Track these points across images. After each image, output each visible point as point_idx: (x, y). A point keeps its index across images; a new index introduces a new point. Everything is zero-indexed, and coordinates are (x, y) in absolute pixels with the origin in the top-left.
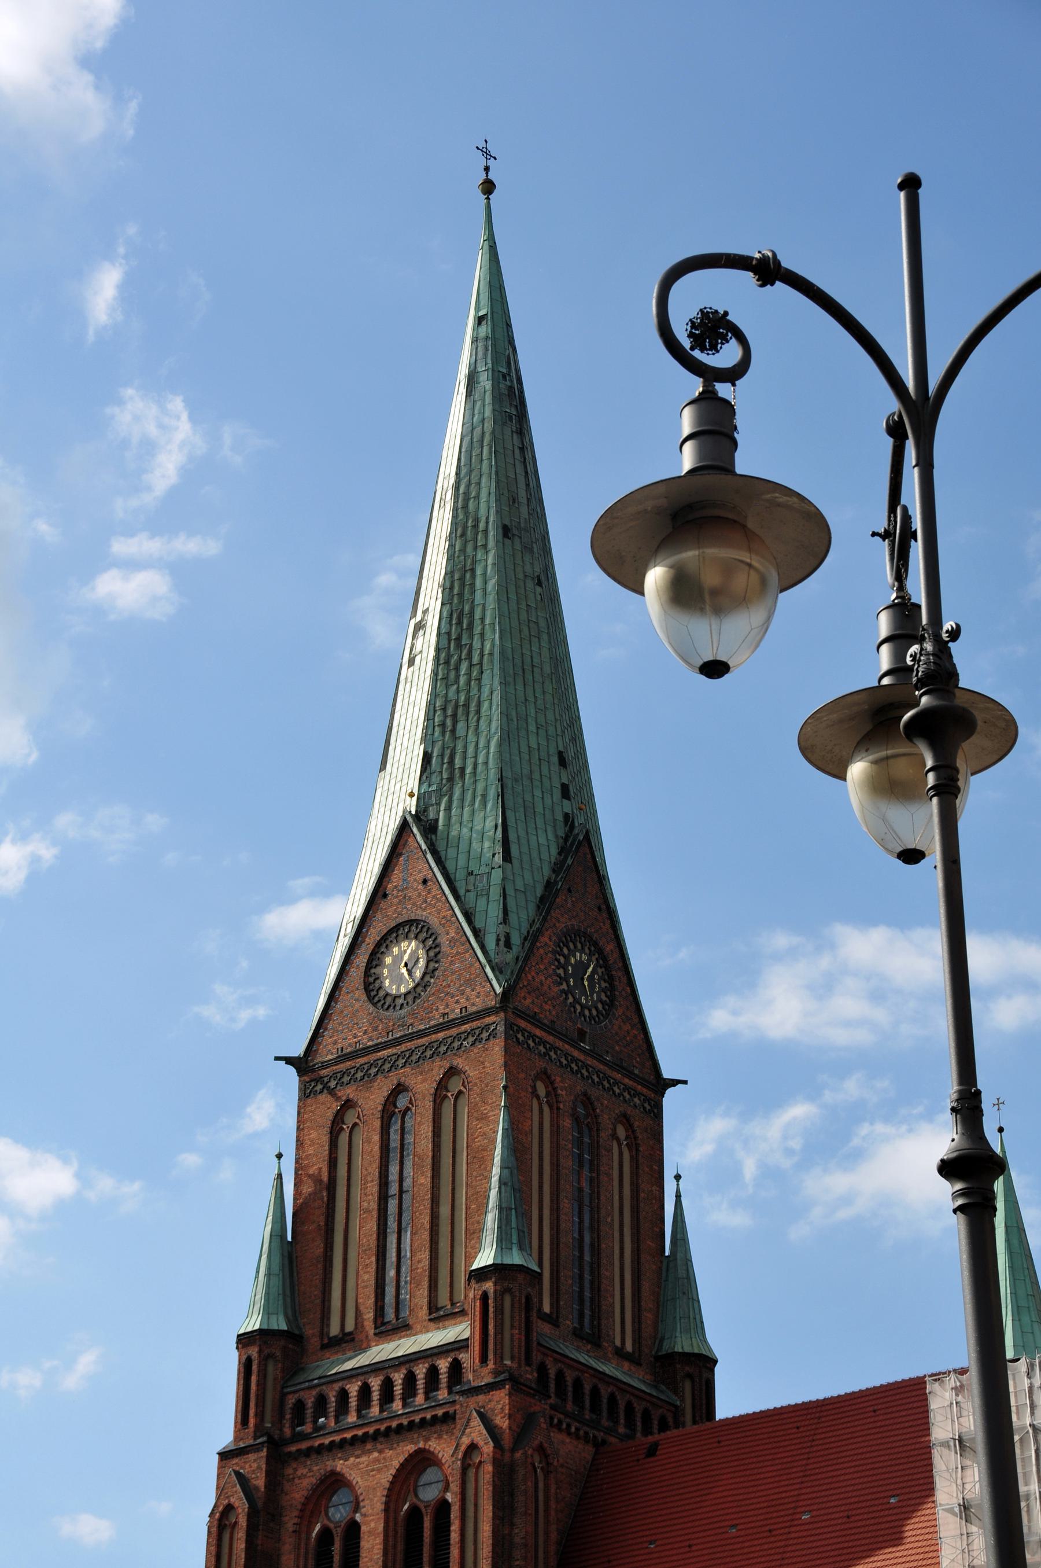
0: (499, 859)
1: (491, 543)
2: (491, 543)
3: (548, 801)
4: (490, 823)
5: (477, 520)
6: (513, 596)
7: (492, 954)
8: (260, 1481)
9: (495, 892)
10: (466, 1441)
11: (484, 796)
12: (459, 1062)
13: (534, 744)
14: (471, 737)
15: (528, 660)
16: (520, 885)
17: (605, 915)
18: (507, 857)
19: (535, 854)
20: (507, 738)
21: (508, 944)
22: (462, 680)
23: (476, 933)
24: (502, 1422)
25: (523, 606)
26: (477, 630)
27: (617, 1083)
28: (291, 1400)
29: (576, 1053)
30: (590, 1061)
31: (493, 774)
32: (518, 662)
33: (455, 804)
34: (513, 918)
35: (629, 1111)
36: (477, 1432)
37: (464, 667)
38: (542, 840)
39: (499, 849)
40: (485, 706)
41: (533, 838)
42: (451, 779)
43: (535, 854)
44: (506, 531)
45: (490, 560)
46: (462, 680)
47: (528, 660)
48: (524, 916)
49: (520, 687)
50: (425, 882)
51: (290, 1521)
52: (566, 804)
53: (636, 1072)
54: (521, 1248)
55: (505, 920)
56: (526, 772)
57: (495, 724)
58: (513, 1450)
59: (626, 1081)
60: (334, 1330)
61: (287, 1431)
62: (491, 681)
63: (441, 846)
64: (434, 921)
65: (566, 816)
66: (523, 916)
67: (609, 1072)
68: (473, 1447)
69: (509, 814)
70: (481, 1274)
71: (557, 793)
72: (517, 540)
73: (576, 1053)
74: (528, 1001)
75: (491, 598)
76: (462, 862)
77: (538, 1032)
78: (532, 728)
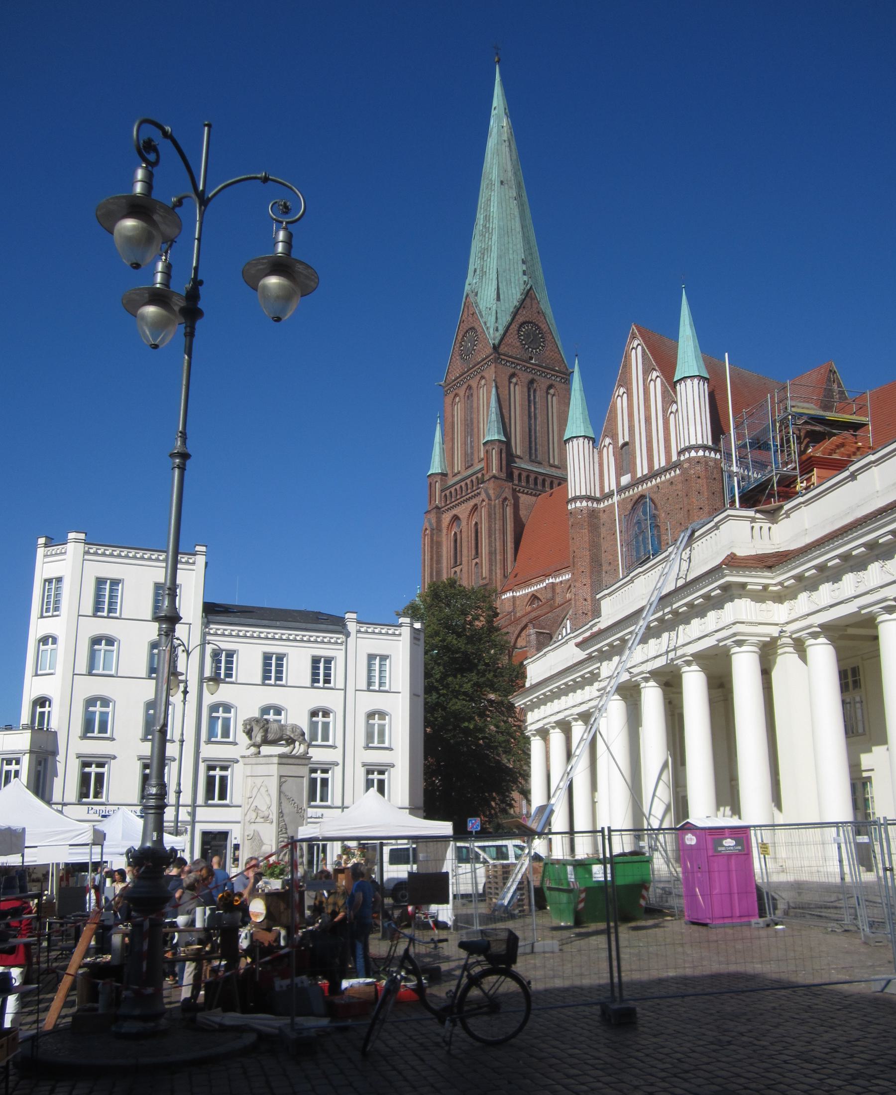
0: (495, 301)
1: (496, 189)
2: (496, 189)
3: (517, 278)
4: (493, 289)
5: (491, 180)
6: (504, 206)
7: (492, 335)
8: (434, 521)
9: (494, 312)
10: (481, 499)
11: (492, 280)
12: (483, 374)
13: (511, 257)
14: (489, 260)
15: (509, 227)
16: (503, 309)
17: (541, 315)
18: (498, 299)
19: (510, 297)
20: (500, 257)
21: (497, 330)
22: (487, 239)
23: (487, 328)
24: (491, 492)
25: (508, 209)
26: (491, 221)
27: (548, 374)
28: (443, 494)
29: (528, 365)
30: (534, 367)
31: (495, 271)
32: (506, 229)
33: (484, 284)
34: (499, 321)
35: (554, 383)
36: (483, 495)
37: (487, 235)
38: (514, 292)
39: (496, 296)
40: (493, 247)
41: (510, 292)
42: (482, 276)
43: (510, 297)
44: (502, 183)
45: (496, 194)
46: (487, 239)
47: (509, 227)
48: (504, 319)
49: (506, 238)
50: (473, 314)
51: (444, 531)
52: (525, 278)
53: (557, 368)
54: (499, 433)
55: (496, 322)
56: (507, 268)
57: (496, 253)
58: (495, 500)
59: (552, 372)
60: (456, 471)
61: (443, 504)
62: (495, 237)
63: (478, 301)
64: (476, 327)
65: (525, 281)
66: (505, 319)
67: (544, 370)
68: (483, 501)
69: (500, 284)
70: (485, 444)
71: (521, 273)
72: (506, 185)
73: (528, 365)
74: (506, 349)
75: (496, 208)
76: (484, 304)
77: (510, 359)
78: (511, 252)
